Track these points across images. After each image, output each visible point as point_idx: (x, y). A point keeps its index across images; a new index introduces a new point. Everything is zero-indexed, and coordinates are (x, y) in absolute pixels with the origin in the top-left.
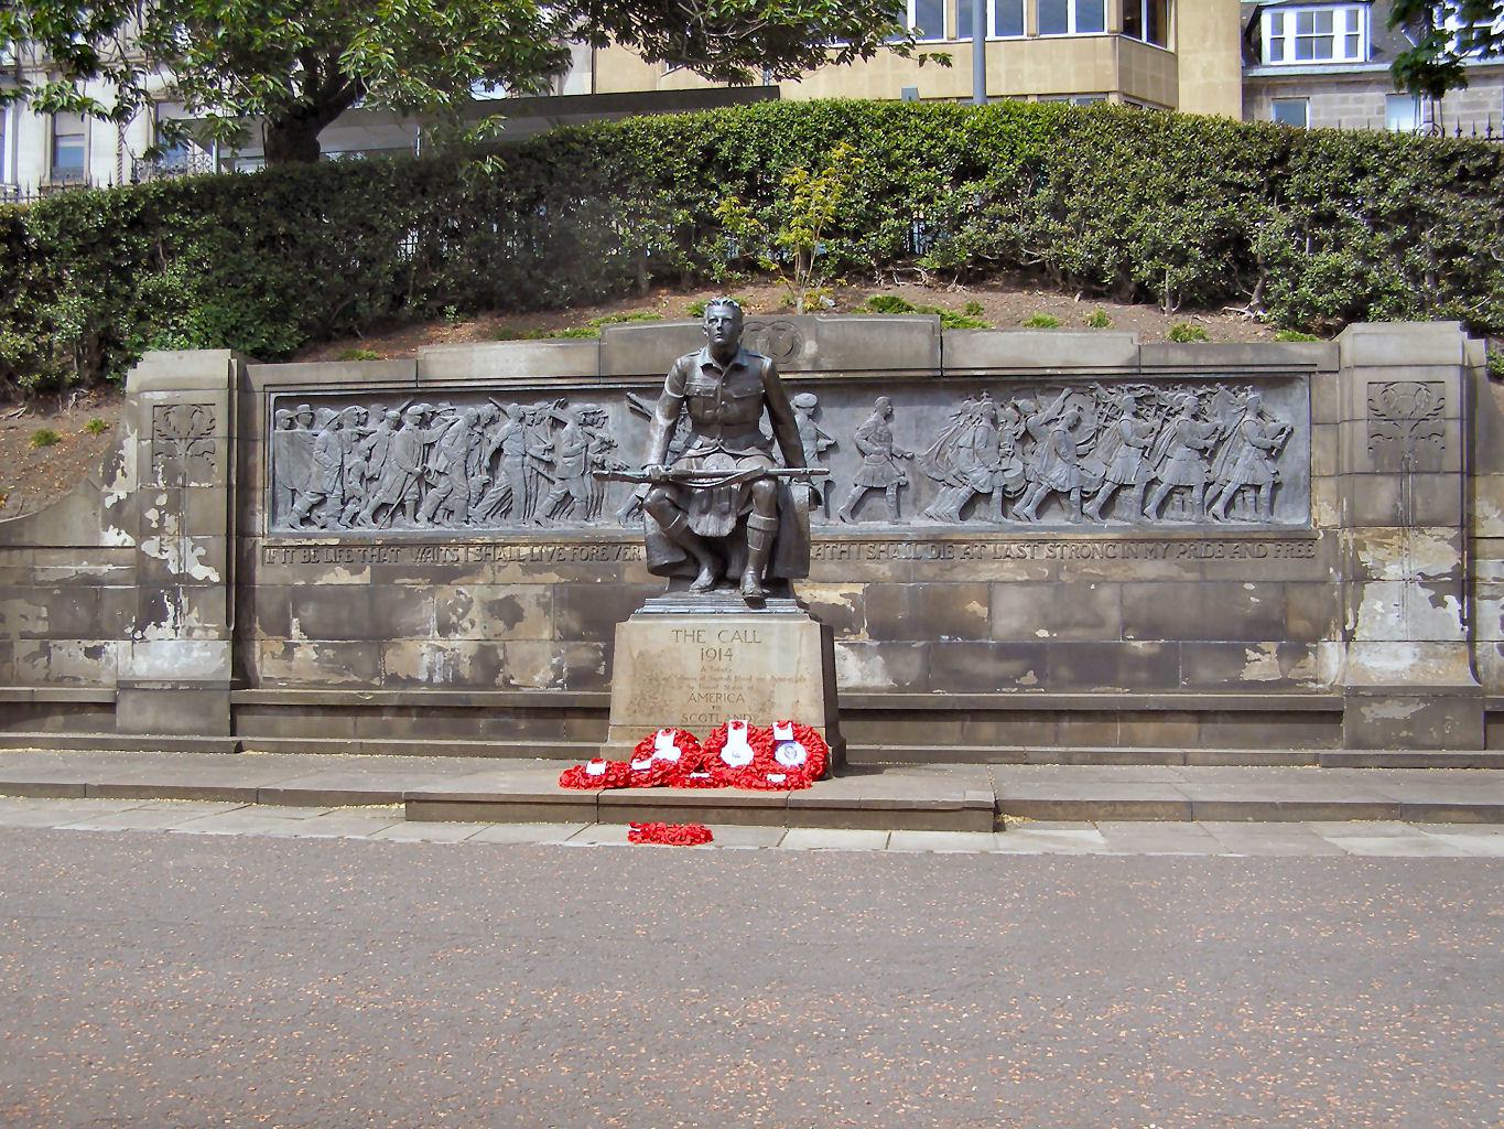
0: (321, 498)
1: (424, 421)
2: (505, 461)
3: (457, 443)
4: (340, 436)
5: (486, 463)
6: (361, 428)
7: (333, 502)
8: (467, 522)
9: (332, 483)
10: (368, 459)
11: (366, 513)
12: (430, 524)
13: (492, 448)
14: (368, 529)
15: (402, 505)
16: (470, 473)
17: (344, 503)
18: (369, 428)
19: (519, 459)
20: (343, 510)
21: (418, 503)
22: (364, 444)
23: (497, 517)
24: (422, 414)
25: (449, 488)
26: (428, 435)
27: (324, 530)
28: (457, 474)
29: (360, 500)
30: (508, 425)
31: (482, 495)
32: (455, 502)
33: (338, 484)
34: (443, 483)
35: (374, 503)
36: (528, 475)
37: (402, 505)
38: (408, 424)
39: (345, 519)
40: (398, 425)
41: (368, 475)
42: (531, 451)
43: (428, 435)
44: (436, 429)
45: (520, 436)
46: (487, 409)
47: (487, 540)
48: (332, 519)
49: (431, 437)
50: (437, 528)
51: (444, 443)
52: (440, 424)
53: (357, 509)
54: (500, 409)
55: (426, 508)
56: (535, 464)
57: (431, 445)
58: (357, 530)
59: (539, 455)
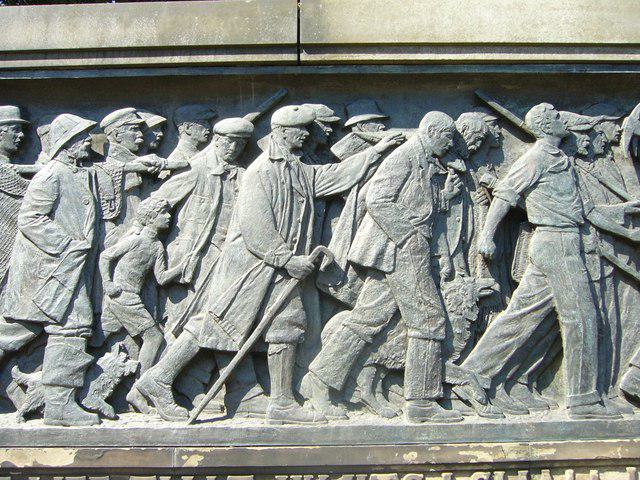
0: (28, 334)
1: (315, 146)
2: (532, 245)
3: (405, 195)
4: (93, 180)
5: (484, 242)
6: (151, 158)
7: (62, 351)
8: (443, 401)
9: (66, 294)
10: (166, 234)
11: (156, 376)
12: (340, 409)
13: (497, 209)
14: (154, 421)
15: (257, 356)
16: (444, 270)
17: (97, 343)
18: (173, 160)
19: (572, 235)
20: (91, 371)
21: (304, 349)
22: (159, 197)
23: (519, 388)
24: (310, 126)
25: (389, 308)
26: (325, 178)
27: (36, 424)
28: (408, 274)
29: (139, 340)
30: (523, 161)
31: (478, 328)
32: (411, 348)
33: (82, 300)
34: (369, 298)
35: (177, 348)
36: (596, 276)
37: (257, 356)
38: (272, 145)
39: (96, 398)
40: (245, 151)
41: (162, 276)
42: (596, 218)
43: (325, 178)
44: (349, 162)
45: (567, 179)
46: (472, 122)
47: (510, 451)
48: (58, 392)
49: (336, 180)
50: (357, 418)
51: (372, 192)
52: (357, 149)
53: (130, 367)
54: (502, 121)
55: (324, 365)
56: (607, 249)
57: (335, 202)
58: (129, 421)
59: (617, 225)
